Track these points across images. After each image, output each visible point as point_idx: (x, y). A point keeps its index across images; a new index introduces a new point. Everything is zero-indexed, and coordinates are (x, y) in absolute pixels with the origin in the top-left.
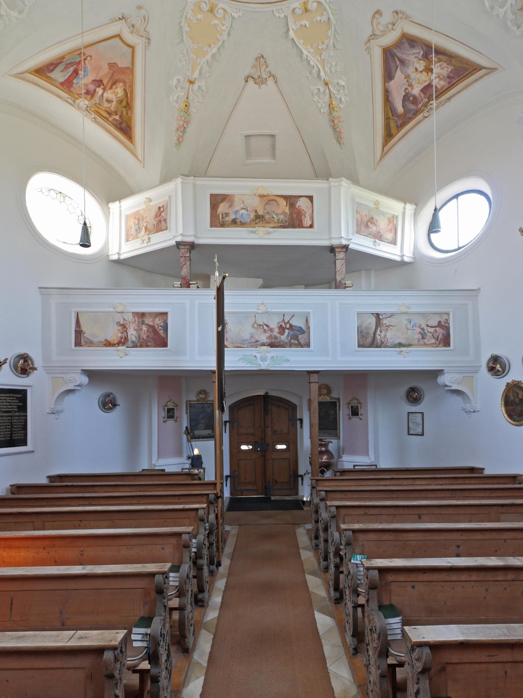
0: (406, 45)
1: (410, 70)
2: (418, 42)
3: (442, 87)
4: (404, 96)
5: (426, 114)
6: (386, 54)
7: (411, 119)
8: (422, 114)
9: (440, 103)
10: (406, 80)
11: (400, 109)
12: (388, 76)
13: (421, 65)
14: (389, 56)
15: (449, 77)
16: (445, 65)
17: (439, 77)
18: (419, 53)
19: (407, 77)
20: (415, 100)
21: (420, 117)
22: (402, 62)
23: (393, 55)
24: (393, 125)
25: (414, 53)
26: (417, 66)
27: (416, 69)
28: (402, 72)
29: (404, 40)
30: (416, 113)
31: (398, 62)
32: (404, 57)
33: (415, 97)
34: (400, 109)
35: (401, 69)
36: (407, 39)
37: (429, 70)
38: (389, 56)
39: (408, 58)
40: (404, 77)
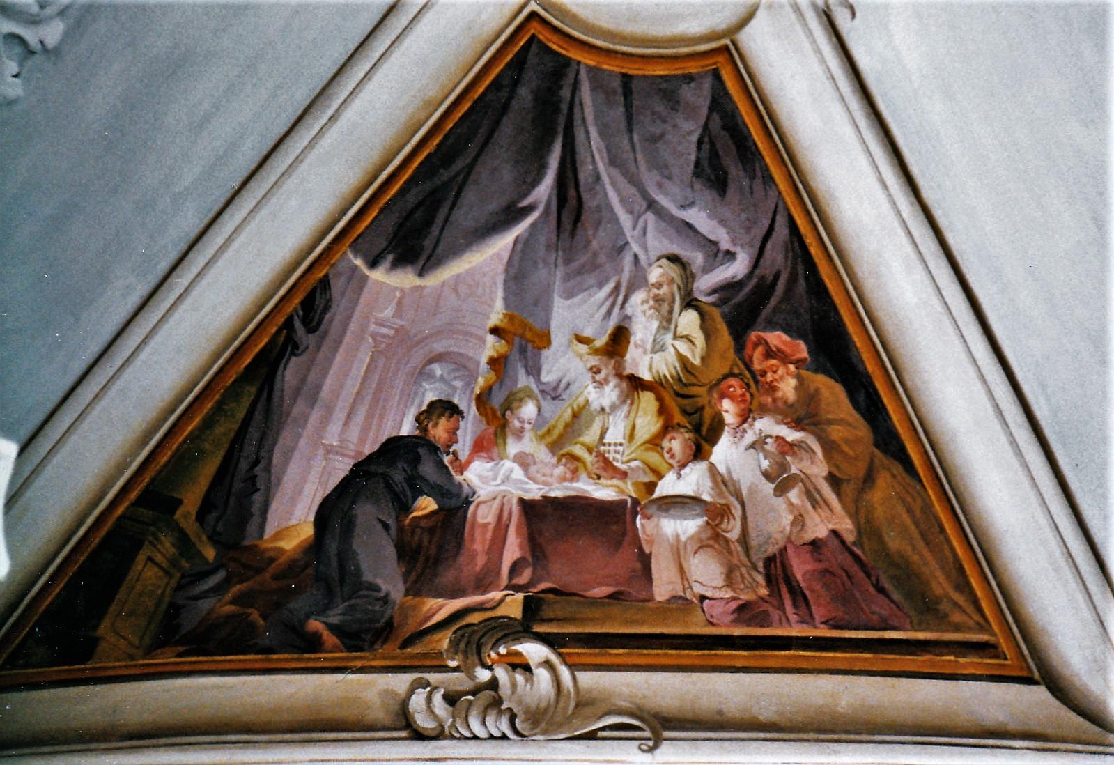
0: (684, 136)
1: (575, 315)
2: (768, 179)
3: (681, 604)
4: (394, 448)
5: (426, 708)
6: (519, 63)
7: (298, 648)
8: (399, 682)
9: (586, 704)
10: (492, 346)
11: (291, 518)
12: (411, 213)
13: (665, 344)
14: (524, 94)
15: (776, 569)
16: (818, 469)
17: (716, 514)
18: (717, 255)
19: (523, 338)
20: (436, 546)
21: (374, 688)
22: (571, 208)
23: (552, 120)
24: (148, 575)
25: (688, 228)
26: (644, 328)
27: (619, 339)
28: (518, 273)
29: (698, 97)
30: (371, 636)
31: (544, 190)
32: (613, 193)
33: (455, 507)
34: (291, 518)
35: (522, 248)
36: (720, 102)
37: (690, 417)
38: (524, 94)
39: (625, 219)
40: (495, 319)
